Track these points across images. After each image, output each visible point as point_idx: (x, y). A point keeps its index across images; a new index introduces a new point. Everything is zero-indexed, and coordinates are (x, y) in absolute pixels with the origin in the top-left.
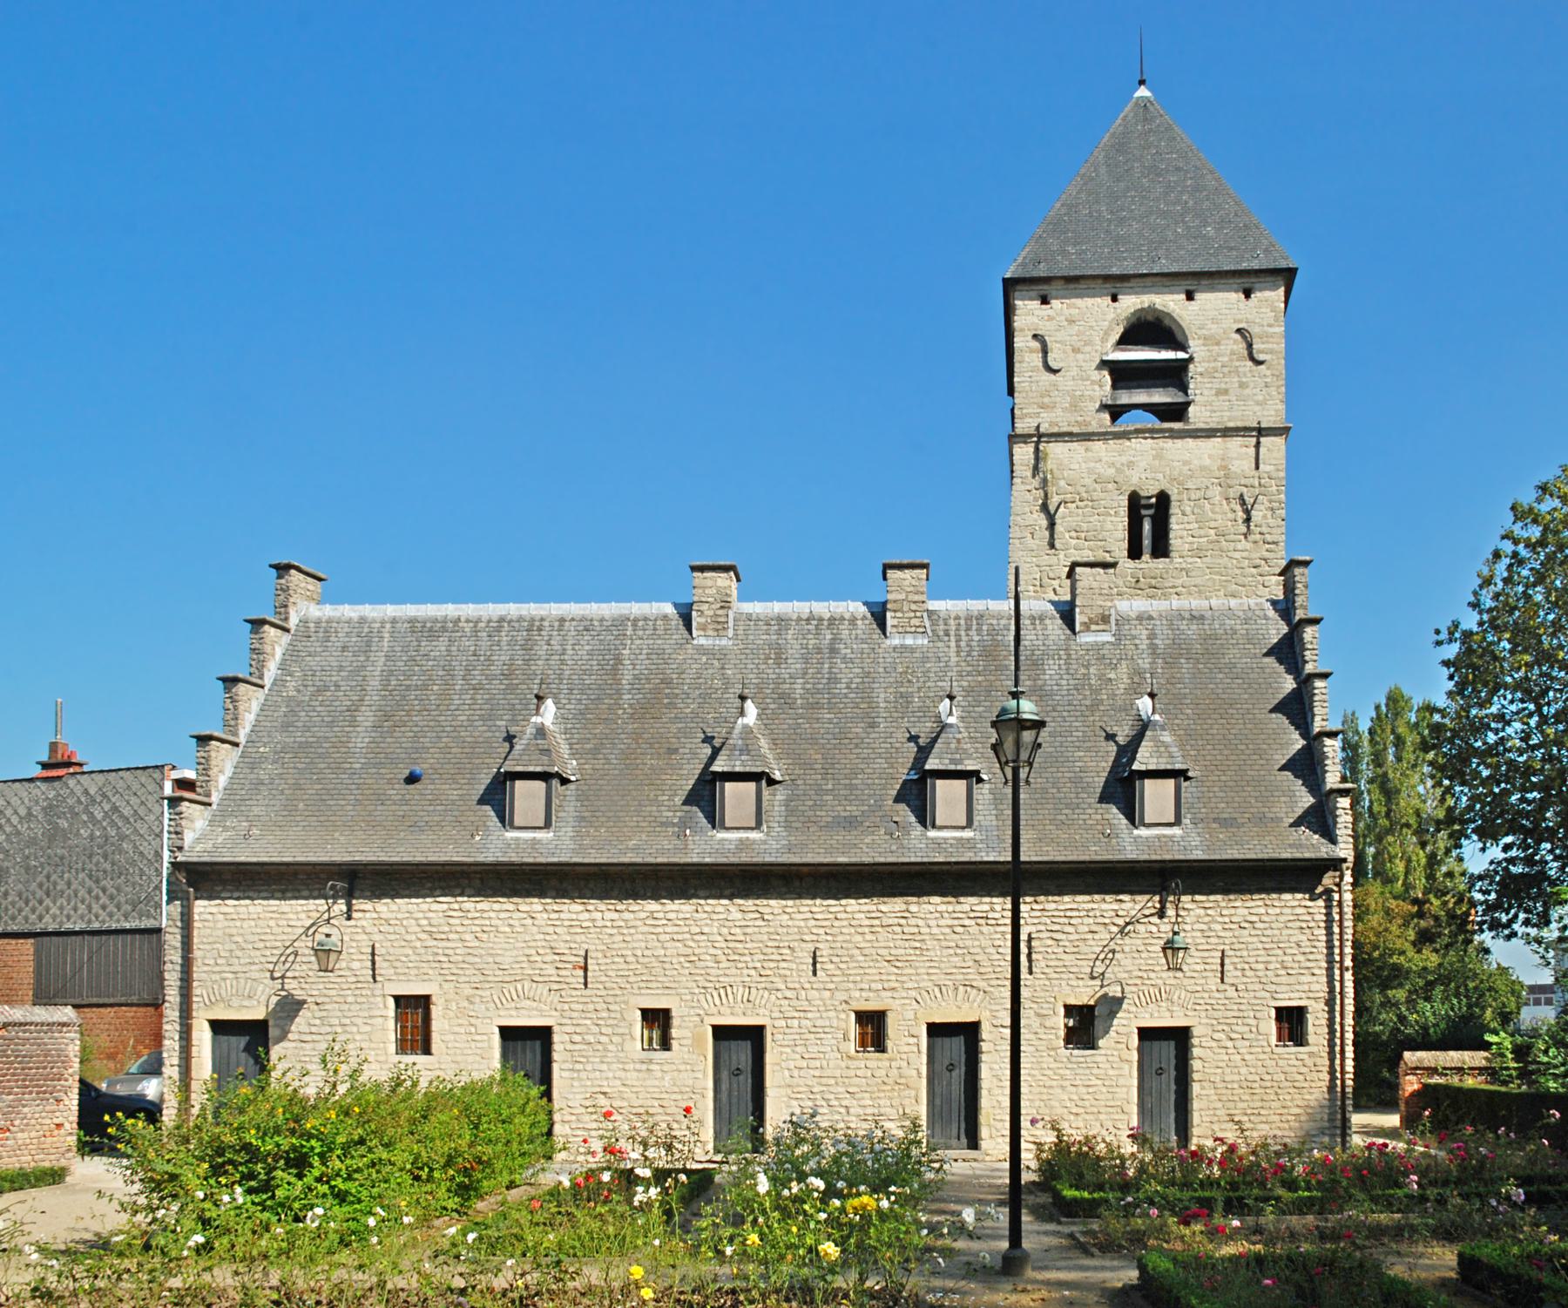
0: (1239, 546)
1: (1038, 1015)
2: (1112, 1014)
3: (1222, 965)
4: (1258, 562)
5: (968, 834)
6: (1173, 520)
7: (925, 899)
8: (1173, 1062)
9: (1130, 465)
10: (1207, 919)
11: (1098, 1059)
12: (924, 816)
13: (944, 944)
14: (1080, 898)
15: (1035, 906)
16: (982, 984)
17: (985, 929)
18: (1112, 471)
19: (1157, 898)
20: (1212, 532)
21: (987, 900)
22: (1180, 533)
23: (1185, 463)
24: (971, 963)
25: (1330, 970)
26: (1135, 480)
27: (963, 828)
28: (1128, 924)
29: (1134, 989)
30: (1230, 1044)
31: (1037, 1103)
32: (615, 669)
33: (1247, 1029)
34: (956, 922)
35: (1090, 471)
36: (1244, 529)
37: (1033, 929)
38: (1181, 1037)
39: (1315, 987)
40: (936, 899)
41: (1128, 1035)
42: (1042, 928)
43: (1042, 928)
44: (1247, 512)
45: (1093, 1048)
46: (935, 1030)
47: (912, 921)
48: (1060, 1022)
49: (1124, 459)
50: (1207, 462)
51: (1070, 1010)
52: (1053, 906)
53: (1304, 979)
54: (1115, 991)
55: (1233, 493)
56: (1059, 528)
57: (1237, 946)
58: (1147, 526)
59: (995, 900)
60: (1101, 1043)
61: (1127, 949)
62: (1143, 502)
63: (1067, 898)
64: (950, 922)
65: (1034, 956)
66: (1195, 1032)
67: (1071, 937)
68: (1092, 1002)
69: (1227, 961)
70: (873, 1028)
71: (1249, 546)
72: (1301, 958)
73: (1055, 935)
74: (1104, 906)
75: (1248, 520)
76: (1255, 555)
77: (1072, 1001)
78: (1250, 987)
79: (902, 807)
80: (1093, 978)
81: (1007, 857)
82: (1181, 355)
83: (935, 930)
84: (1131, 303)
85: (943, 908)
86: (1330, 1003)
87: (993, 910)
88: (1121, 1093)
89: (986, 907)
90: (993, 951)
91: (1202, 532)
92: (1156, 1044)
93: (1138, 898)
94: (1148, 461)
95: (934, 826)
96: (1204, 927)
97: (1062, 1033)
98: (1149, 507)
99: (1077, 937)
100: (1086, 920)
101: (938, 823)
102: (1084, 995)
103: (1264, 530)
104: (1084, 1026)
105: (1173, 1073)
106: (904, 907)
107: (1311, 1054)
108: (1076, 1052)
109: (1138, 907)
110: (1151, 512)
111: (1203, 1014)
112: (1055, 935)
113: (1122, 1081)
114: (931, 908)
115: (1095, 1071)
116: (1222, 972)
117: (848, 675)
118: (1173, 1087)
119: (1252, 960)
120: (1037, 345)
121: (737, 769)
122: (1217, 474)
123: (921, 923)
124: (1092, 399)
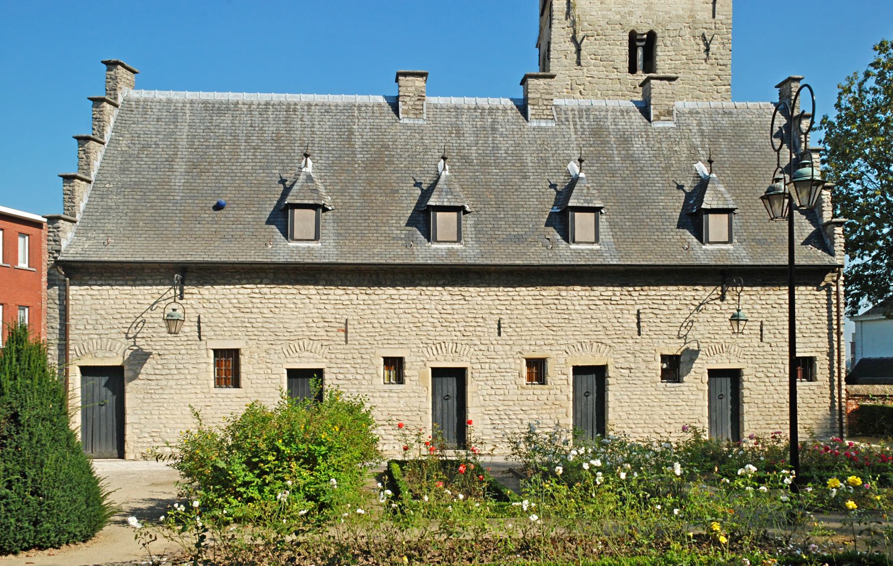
0: (702, 67)
1: (644, 361)
2: (692, 361)
3: (761, 330)
4: (714, 77)
5: (596, 247)
6: (658, 49)
7: (571, 288)
8: (729, 391)
9: (631, 13)
10: (751, 302)
11: (683, 389)
12: (567, 234)
13: (583, 316)
14: (670, 288)
15: (642, 293)
16: (609, 342)
17: (610, 307)
18: (618, 17)
19: (719, 288)
20: (684, 57)
21: (611, 288)
22: (663, 58)
23: (667, 13)
24: (601, 329)
25: (830, 335)
26: (633, 23)
27: (593, 243)
28: (701, 304)
29: (706, 345)
30: (767, 380)
31: (644, 417)
33: (777, 370)
34: (591, 302)
35: (604, 17)
36: (705, 56)
37: (640, 307)
38: (735, 376)
39: (820, 345)
40: (578, 288)
41: (702, 374)
42: (647, 306)
43: (647, 306)
44: (707, 45)
45: (679, 382)
46: (578, 371)
47: (563, 302)
48: (658, 365)
49: (626, 10)
50: (681, 13)
51: (664, 358)
52: (654, 293)
53: (813, 340)
54: (693, 346)
55: (698, 33)
57: (770, 319)
58: (640, 53)
59: (616, 289)
60: (685, 379)
61: (701, 320)
62: (638, 37)
63: (662, 288)
64: (587, 302)
65: (641, 324)
66: (745, 372)
67: (665, 312)
68: (679, 353)
69: (764, 328)
70: (537, 369)
71: (708, 66)
72: (811, 326)
73: (655, 311)
74: (686, 293)
75: (707, 50)
76: (711, 73)
77: (666, 352)
78: (779, 344)
79: (551, 229)
80: (679, 338)
83: (578, 307)
85: (582, 293)
86: (830, 354)
87: (614, 295)
88: (698, 410)
89: (610, 293)
90: (615, 320)
91: (678, 57)
92: (718, 379)
93: (707, 288)
95: (574, 242)
96: (750, 307)
97: (660, 372)
99: (669, 312)
100: (675, 302)
101: (576, 240)
102: (674, 349)
103: (718, 56)
104: (674, 368)
105: (730, 398)
106: (557, 293)
107: (819, 387)
108: (669, 384)
109: (707, 294)
110: (643, 44)
111: (750, 361)
112: (655, 311)
113: (698, 403)
114: (575, 293)
115: (682, 396)
116: (761, 335)
117: (505, 145)
118: (730, 407)
119: (780, 327)
121: (445, 204)
122: (687, 20)
123: (568, 302)
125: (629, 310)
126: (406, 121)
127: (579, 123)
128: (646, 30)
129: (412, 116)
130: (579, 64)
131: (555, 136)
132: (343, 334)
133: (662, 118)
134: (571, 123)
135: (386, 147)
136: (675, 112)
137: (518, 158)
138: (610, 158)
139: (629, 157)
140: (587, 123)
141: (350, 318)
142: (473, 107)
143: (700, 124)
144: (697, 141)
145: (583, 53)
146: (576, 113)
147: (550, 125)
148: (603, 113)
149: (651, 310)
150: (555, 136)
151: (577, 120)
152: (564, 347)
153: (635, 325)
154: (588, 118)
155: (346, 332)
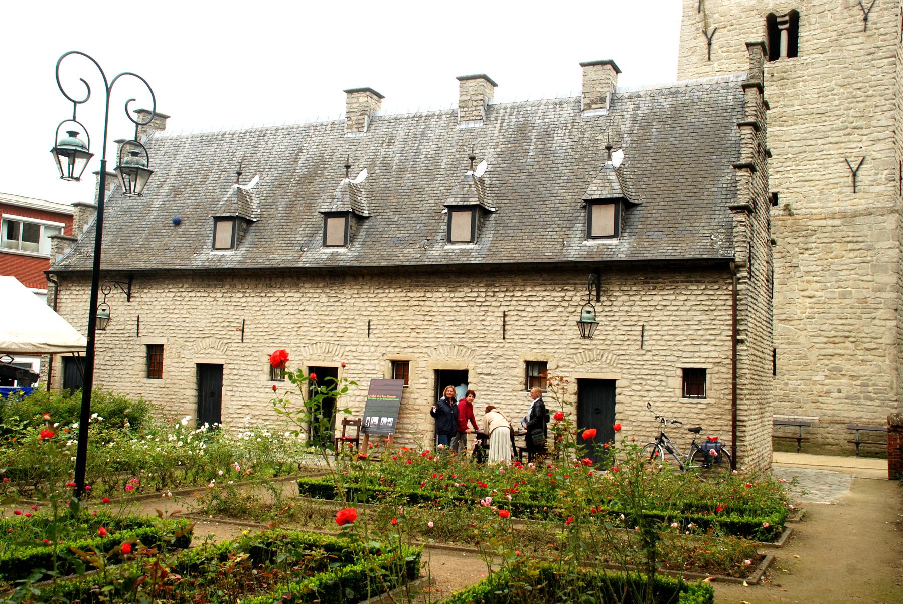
5: (471, 246)
20: (835, 33)
27: (468, 242)
32: (297, 155)
37: (506, 309)
48: (520, 371)
56: (715, 46)
58: (784, 36)
62: (779, 20)
74: (555, 294)
75: (866, 19)
85: (447, 294)
114: (440, 295)
117: (428, 149)
121: (333, 210)
125: (493, 312)
126: (349, 135)
127: (507, 121)
128: (787, 10)
129: (355, 130)
130: (709, 59)
132: (240, 333)
133: (594, 106)
134: (499, 122)
135: (323, 161)
136: (608, 100)
137: (435, 160)
138: (525, 154)
139: (545, 152)
140: (514, 120)
141: (246, 318)
142: (411, 116)
143: (637, 108)
146: (508, 111)
147: (477, 125)
148: (534, 108)
149: (516, 313)
151: (506, 118)
152: (425, 350)
153: (499, 328)
155: (243, 332)
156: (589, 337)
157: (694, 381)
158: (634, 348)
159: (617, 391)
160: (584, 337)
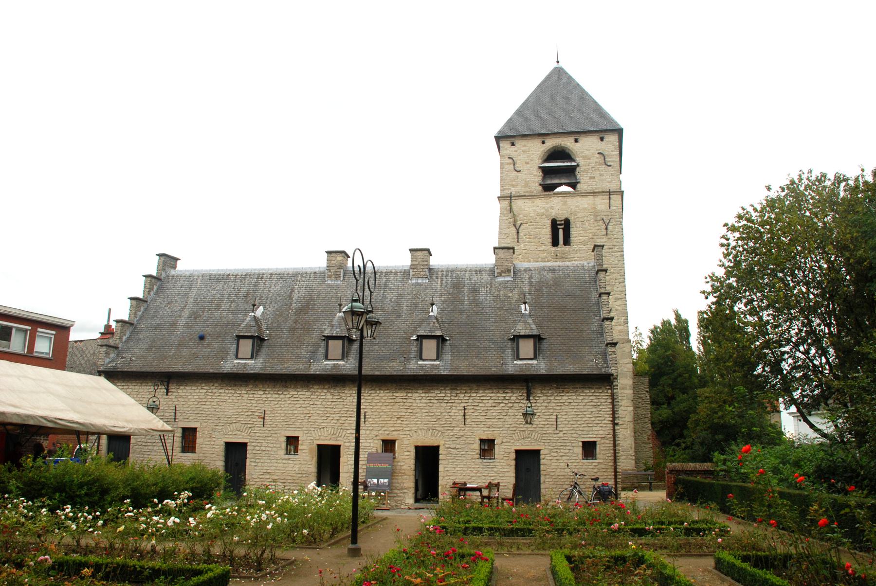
5: (437, 363)
9: (552, 208)
18: (543, 211)
23: (577, 206)
26: (553, 214)
27: (434, 360)
32: (291, 293)
35: (535, 211)
48: (477, 446)
50: (586, 206)
58: (561, 232)
81: (356, 373)
82: (573, 164)
84: (551, 143)
94: (559, 205)
98: (561, 225)
120: (511, 161)
124: (534, 182)
126: (329, 282)
128: (563, 218)
131: (426, 289)
135: (312, 299)
138: (462, 302)
139: (475, 302)
143: (531, 278)
144: (526, 289)
145: (521, 234)
150: (426, 289)
152: (408, 432)
154: (452, 276)
156: (530, 423)
157: (589, 449)
158: (551, 430)
159: (542, 457)
160: (527, 423)
